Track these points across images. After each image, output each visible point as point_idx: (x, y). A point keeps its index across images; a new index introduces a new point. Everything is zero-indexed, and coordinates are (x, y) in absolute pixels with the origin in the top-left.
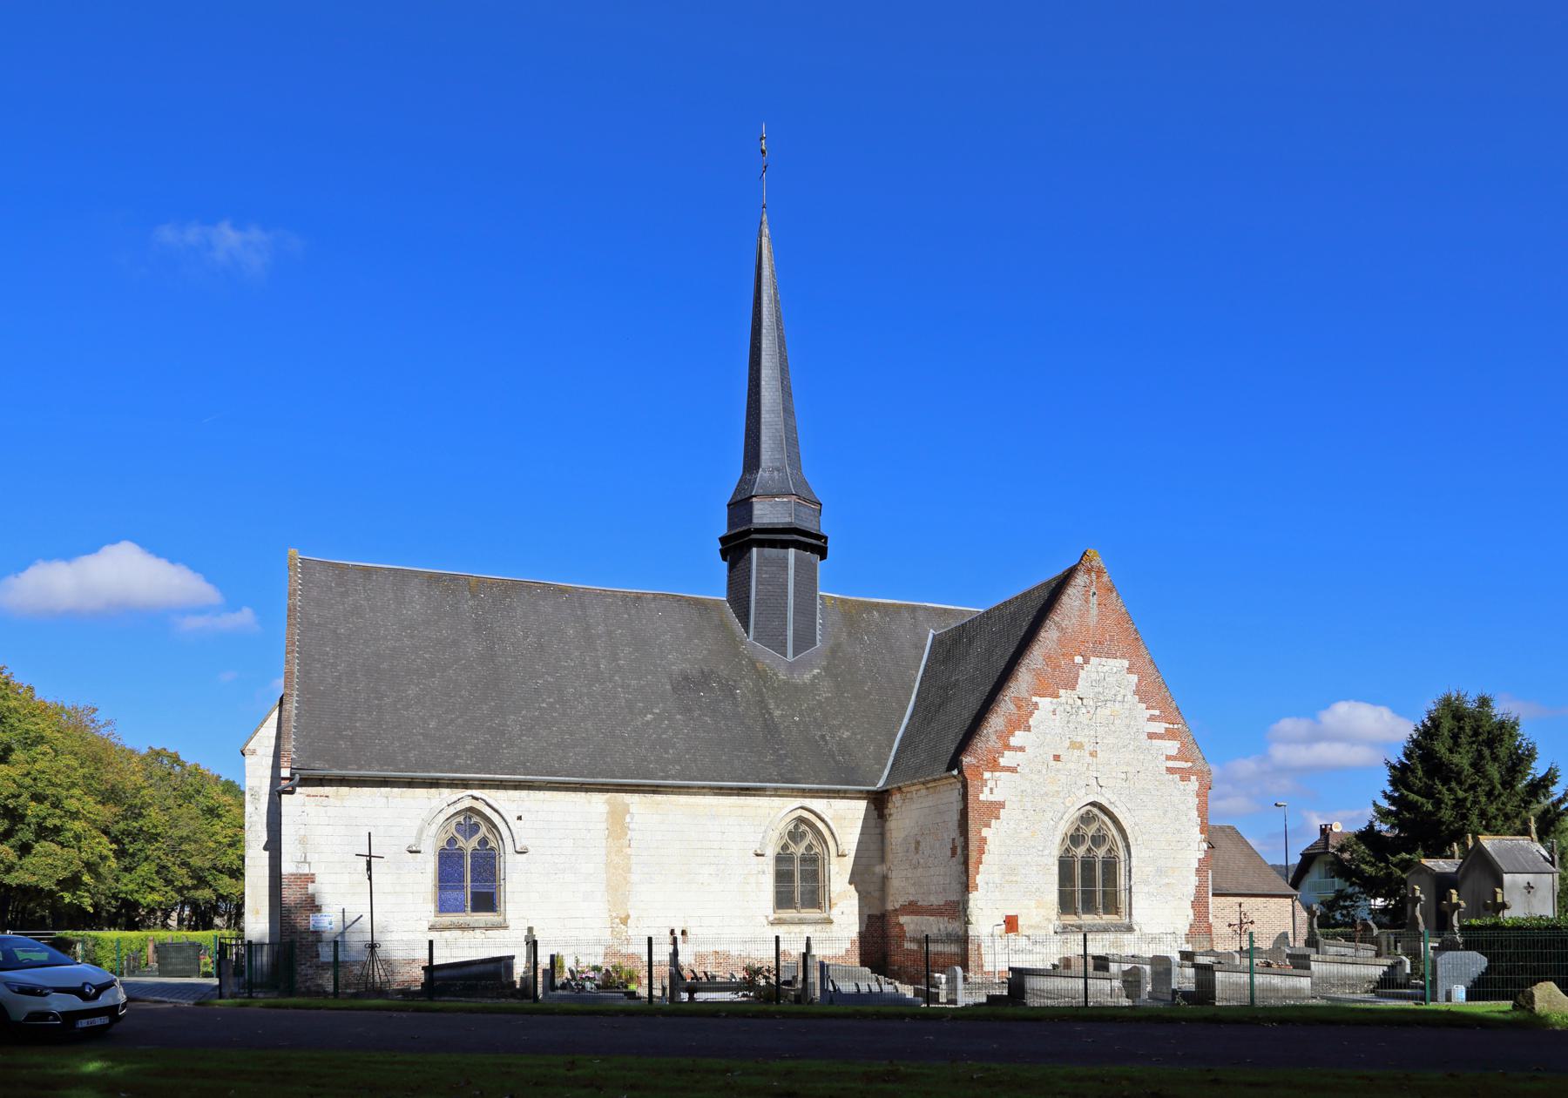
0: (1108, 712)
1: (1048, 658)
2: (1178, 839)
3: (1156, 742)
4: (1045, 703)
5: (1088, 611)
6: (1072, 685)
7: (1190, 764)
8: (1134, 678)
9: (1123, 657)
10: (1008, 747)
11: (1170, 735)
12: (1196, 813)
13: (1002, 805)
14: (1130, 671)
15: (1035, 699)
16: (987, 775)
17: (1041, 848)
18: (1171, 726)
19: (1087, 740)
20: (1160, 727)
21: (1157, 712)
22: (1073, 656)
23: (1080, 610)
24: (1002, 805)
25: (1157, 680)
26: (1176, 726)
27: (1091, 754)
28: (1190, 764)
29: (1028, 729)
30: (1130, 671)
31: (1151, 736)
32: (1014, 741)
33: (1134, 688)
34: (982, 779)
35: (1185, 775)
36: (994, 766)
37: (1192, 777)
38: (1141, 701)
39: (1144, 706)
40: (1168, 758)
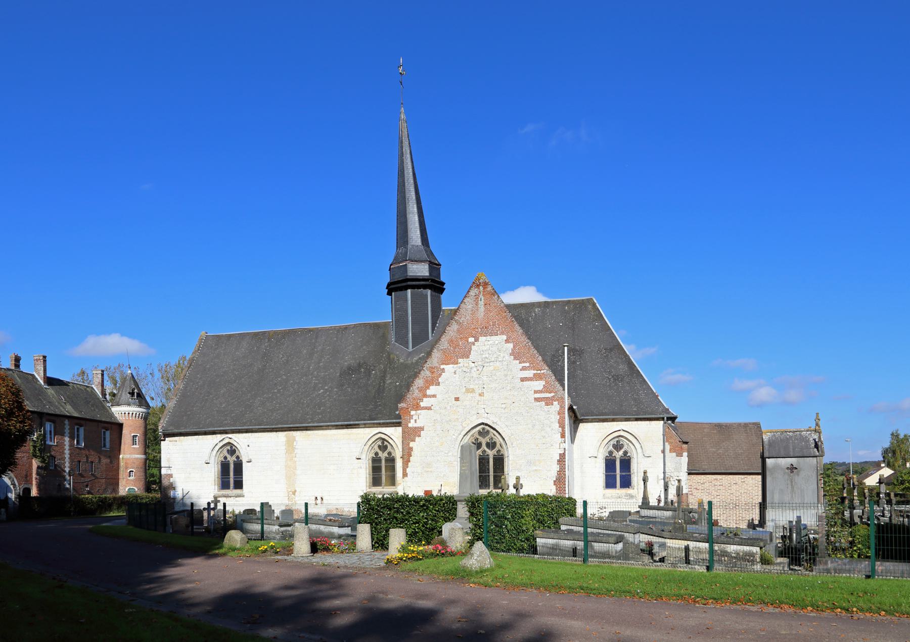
0: (492, 368)
1: (451, 341)
2: (544, 442)
3: (526, 383)
4: (449, 368)
5: (477, 310)
6: (466, 355)
7: (552, 394)
8: (511, 346)
9: (502, 333)
10: (425, 396)
11: (537, 377)
12: (558, 425)
13: (422, 429)
14: (507, 341)
15: (442, 367)
16: (413, 413)
17: (447, 452)
18: (539, 372)
19: (477, 387)
20: (530, 373)
21: (527, 365)
22: (467, 338)
23: (472, 310)
24: (422, 429)
25: (527, 345)
26: (542, 372)
27: (480, 395)
28: (552, 394)
29: (438, 384)
30: (507, 341)
31: (523, 380)
32: (429, 392)
33: (511, 352)
34: (410, 415)
35: (548, 402)
36: (417, 407)
37: (554, 402)
38: (515, 358)
39: (518, 361)
40: (536, 392)
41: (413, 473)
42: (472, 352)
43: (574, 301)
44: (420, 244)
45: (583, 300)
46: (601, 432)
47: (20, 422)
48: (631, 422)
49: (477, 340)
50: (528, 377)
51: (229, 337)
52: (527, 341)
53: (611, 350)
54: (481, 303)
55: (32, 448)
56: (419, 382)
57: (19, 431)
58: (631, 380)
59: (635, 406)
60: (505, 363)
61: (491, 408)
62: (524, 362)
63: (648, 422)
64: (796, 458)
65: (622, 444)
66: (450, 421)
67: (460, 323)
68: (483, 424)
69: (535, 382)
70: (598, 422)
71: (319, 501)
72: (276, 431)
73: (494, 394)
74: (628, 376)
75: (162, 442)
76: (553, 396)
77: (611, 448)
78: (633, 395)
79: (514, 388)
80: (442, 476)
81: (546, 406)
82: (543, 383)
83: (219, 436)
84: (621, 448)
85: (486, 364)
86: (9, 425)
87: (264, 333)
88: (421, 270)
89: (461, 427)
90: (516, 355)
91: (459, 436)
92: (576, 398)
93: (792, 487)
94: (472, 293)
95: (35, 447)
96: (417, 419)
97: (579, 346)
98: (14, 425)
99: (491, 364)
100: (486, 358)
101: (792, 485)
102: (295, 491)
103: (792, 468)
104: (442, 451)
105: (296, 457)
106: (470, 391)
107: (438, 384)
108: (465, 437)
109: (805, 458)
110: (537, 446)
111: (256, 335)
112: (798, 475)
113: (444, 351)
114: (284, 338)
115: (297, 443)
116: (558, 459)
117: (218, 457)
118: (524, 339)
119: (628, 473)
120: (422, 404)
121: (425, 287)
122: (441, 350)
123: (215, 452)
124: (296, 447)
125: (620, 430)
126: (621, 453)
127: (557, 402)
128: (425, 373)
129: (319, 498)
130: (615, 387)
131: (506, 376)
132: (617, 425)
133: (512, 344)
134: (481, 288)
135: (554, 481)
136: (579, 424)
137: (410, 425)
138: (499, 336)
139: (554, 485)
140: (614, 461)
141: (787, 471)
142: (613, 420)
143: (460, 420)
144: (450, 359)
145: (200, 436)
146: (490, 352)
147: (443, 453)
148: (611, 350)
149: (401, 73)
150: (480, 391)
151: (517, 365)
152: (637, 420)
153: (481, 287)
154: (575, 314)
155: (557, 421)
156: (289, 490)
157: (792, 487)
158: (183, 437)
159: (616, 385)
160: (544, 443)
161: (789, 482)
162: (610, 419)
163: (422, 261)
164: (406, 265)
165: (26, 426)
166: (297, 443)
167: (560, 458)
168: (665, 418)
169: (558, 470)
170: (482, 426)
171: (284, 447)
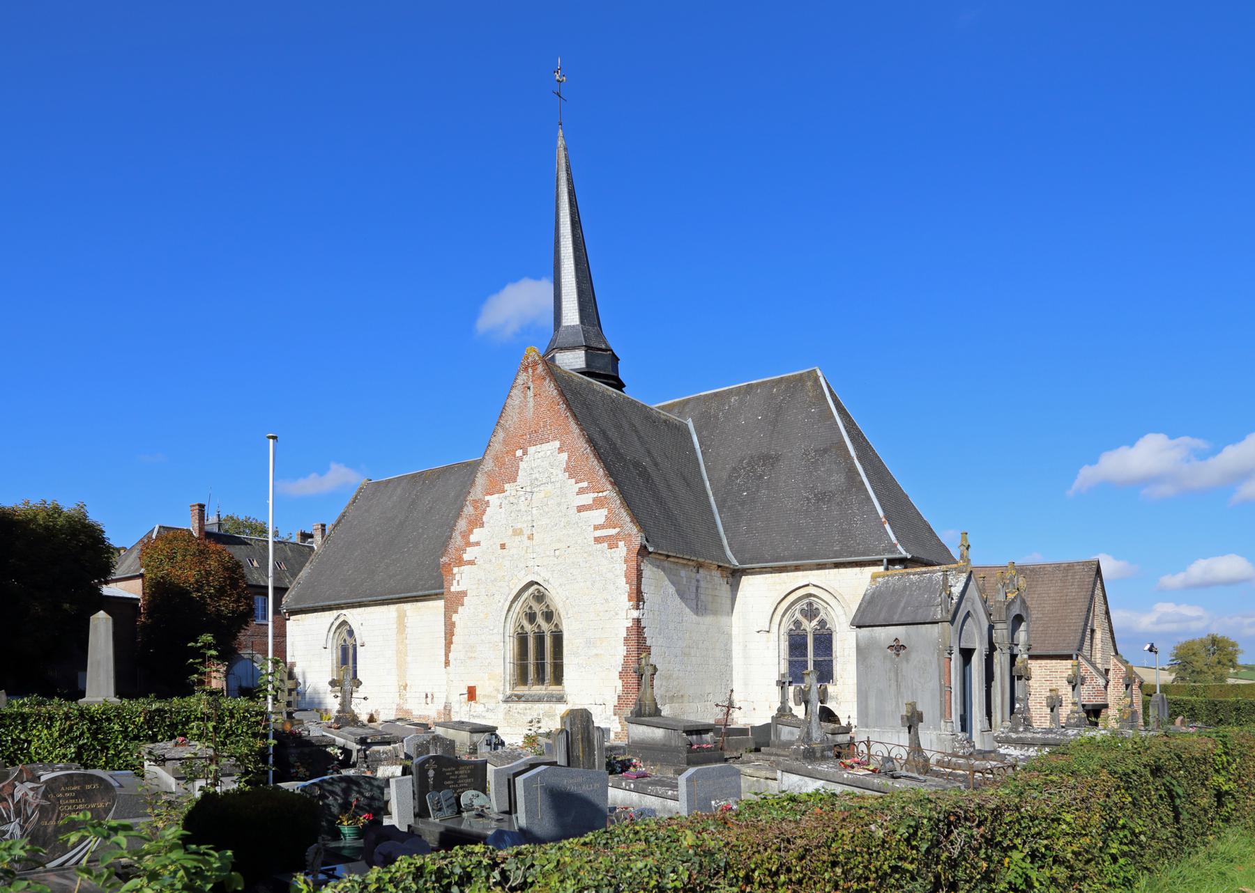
0: (542, 495)
1: (496, 458)
2: (606, 609)
3: (585, 514)
4: (493, 499)
5: (525, 406)
6: (513, 479)
7: (617, 530)
8: (565, 456)
9: (555, 438)
10: (469, 544)
11: (598, 504)
12: (624, 580)
13: (464, 593)
14: (561, 450)
15: (487, 498)
16: (455, 570)
17: (492, 628)
18: (600, 494)
19: (525, 526)
20: (588, 499)
21: (585, 484)
22: (514, 451)
23: (520, 407)
24: (464, 593)
25: (585, 452)
26: (605, 494)
27: (529, 538)
28: (617, 530)
29: (482, 525)
30: (561, 450)
31: (581, 509)
32: (473, 538)
33: (565, 466)
34: (452, 574)
35: (612, 542)
36: (460, 562)
37: (620, 543)
38: (571, 477)
39: (573, 480)
40: (596, 528)
41: (455, 660)
42: (519, 471)
43: (788, 379)
44: (578, 323)
45: (801, 375)
46: (776, 590)
47: (233, 602)
48: (827, 571)
49: (525, 453)
50: (586, 504)
52: (585, 445)
53: (825, 451)
54: (530, 393)
56: (462, 524)
57: (233, 612)
58: (845, 499)
59: (840, 542)
60: (558, 485)
61: (542, 557)
62: (581, 481)
63: (857, 570)
64: (904, 627)
65: (817, 609)
66: (495, 580)
67: (507, 429)
68: (532, 583)
69: (595, 511)
70: (771, 573)
71: (429, 699)
72: (388, 604)
73: (545, 536)
74: (842, 492)
75: (287, 622)
76: (618, 533)
77: (798, 616)
78: (841, 524)
79: (568, 523)
80: (487, 664)
81: (609, 550)
82: (604, 512)
83: (335, 612)
84: (816, 616)
85: (535, 489)
86: (219, 606)
89: (508, 588)
90: (572, 471)
91: (506, 604)
92: (745, 534)
93: (898, 686)
94: (520, 381)
96: (462, 579)
97: (776, 450)
98: (226, 606)
99: (542, 488)
100: (537, 479)
101: (897, 682)
102: (406, 685)
103: (898, 648)
104: (487, 627)
105: (406, 639)
106: (517, 532)
107: (482, 525)
108: (514, 605)
109: (920, 626)
110: (598, 615)
111: (414, 476)
112: (907, 661)
114: (439, 479)
115: (407, 620)
116: (625, 636)
117: (337, 640)
118: (582, 445)
119: (802, 659)
120: (466, 557)
122: (486, 472)
123: (332, 633)
124: (407, 625)
125: (808, 585)
126: (815, 622)
127: (623, 542)
128: (469, 510)
129: (429, 695)
130: (815, 514)
131: (559, 504)
132: (803, 576)
133: (566, 453)
134: (530, 370)
135: (620, 673)
136: (741, 577)
137: (453, 589)
138: (551, 443)
139: (620, 678)
140: (805, 637)
141: (889, 651)
142: (797, 568)
143: (507, 578)
144: (495, 487)
145: (319, 613)
146: (540, 470)
147: (487, 630)
148: (825, 451)
149: (558, 81)
150: (529, 532)
152: (837, 565)
153: (530, 370)
154: (784, 399)
155: (623, 573)
156: (401, 684)
157: (898, 686)
158: (304, 615)
160: (607, 611)
161: (892, 674)
162: (790, 566)
164: (553, 356)
165: (242, 606)
166: (407, 620)
167: (628, 635)
168: (885, 560)
169: (625, 655)
170: (536, 586)
171: (395, 626)
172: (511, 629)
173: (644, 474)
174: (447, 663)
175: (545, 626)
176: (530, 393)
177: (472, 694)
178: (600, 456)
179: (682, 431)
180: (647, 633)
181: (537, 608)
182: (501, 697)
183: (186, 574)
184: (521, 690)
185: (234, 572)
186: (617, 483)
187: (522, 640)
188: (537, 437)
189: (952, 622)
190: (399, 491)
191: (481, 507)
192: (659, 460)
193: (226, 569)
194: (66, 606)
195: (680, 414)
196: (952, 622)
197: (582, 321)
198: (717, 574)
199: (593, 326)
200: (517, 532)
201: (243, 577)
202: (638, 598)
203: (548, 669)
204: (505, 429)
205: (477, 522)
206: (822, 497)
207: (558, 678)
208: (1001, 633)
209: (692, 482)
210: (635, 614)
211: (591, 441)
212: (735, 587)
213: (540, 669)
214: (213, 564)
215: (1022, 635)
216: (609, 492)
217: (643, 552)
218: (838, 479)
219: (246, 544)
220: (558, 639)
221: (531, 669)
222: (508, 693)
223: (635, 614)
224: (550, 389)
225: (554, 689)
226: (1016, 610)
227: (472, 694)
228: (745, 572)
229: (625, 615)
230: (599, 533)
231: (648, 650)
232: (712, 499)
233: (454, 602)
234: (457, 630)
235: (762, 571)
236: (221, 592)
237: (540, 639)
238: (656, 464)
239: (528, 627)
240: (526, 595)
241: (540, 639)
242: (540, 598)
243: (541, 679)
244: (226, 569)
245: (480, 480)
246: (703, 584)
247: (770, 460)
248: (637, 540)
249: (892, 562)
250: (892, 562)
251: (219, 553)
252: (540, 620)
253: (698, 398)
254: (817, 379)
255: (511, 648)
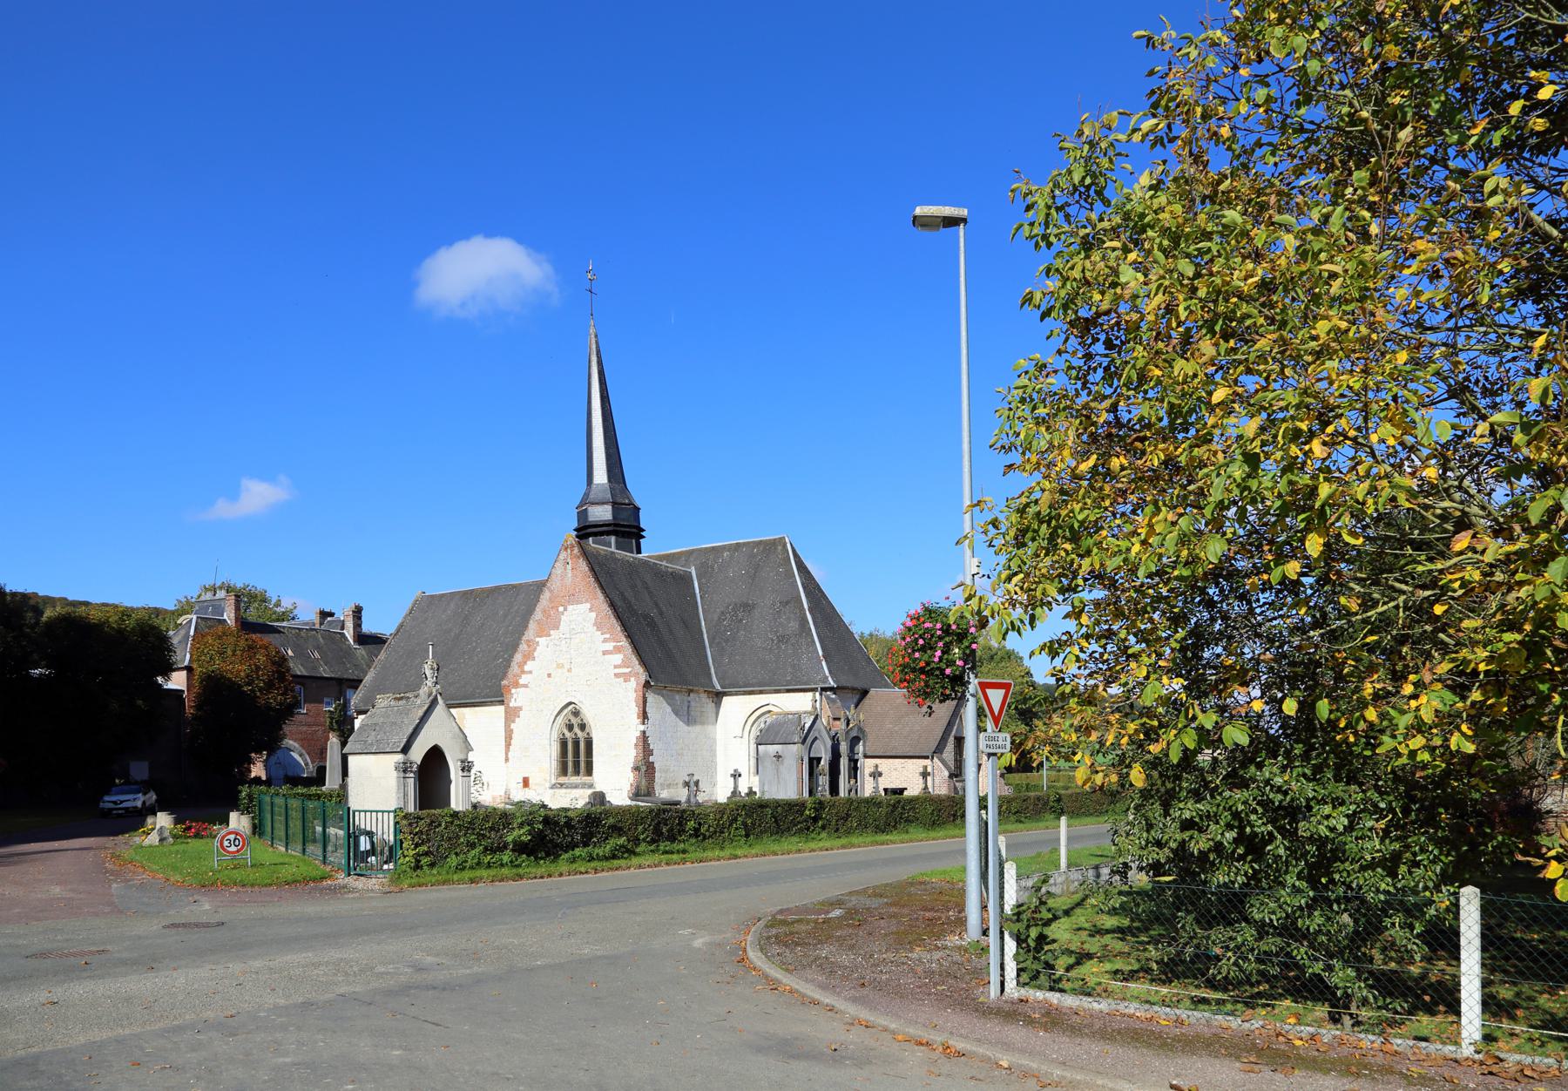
1: (544, 611)
4: (542, 641)
8: (593, 615)
9: (587, 601)
10: (523, 672)
11: (617, 650)
14: (591, 610)
20: (610, 646)
29: (534, 659)
30: (591, 610)
31: (605, 653)
32: (527, 668)
35: (626, 677)
36: (517, 685)
38: (598, 629)
40: (615, 667)
49: (565, 609)
51: (443, 595)
53: (787, 603)
54: (569, 567)
55: (328, 720)
56: (518, 657)
57: (281, 704)
68: (571, 703)
87: (472, 591)
88: (602, 513)
94: (561, 557)
95: (332, 719)
96: (518, 697)
98: (275, 699)
106: (560, 666)
107: (534, 659)
111: (465, 593)
113: (539, 622)
121: (608, 533)
128: (523, 647)
142: (761, 692)
144: (543, 632)
148: (787, 603)
151: (599, 636)
152: (788, 691)
159: (779, 647)
163: (603, 503)
172: (555, 736)
173: (652, 624)
174: (507, 760)
175: (580, 734)
176: (569, 567)
177: (526, 783)
178: (618, 617)
179: (685, 579)
180: (650, 740)
181: (575, 721)
182: (548, 785)
183: (237, 669)
184: (563, 780)
185: (280, 666)
186: (630, 637)
187: (564, 744)
188: (572, 598)
189: (803, 742)
190: (452, 605)
191: (533, 646)
192: (664, 609)
193: (274, 663)
194: (140, 702)
195: (687, 564)
196: (803, 742)
197: (609, 481)
198: (703, 696)
199: (619, 483)
200: (560, 666)
201: (288, 670)
202: (644, 716)
203: (582, 765)
204: (551, 591)
205: (529, 656)
206: (782, 639)
207: (589, 771)
208: (844, 748)
209: (691, 625)
210: (642, 728)
211: (612, 605)
212: (718, 704)
213: (577, 765)
214: (261, 658)
215: (860, 748)
216: (624, 643)
217: (647, 685)
218: (794, 625)
219: (280, 632)
220: (589, 743)
221: (570, 764)
222: (554, 781)
223: (642, 728)
224: (583, 566)
225: (586, 779)
226: (854, 734)
227: (526, 783)
228: (725, 694)
229: (635, 728)
230: (617, 671)
231: (651, 753)
232: (705, 636)
233: (512, 715)
234: (514, 736)
235: (737, 694)
236: (270, 685)
237: (576, 743)
238: (661, 613)
239: (568, 735)
240: (566, 711)
241: (576, 743)
242: (576, 713)
243: (577, 772)
244: (274, 663)
245: (532, 625)
246: (693, 704)
247: (748, 607)
248: (643, 677)
249: (824, 689)
250: (824, 689)
251: (266, 648)
252: (576, 730)
253: (700, 550)
254: (785, 545)
255: (555, 749)
